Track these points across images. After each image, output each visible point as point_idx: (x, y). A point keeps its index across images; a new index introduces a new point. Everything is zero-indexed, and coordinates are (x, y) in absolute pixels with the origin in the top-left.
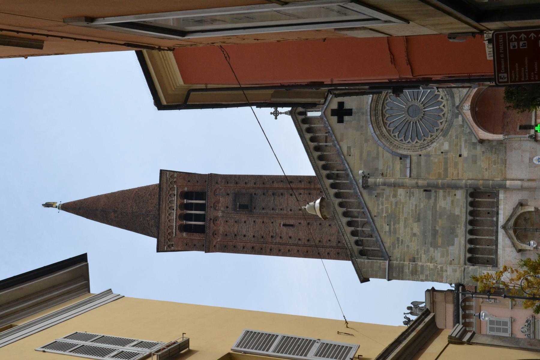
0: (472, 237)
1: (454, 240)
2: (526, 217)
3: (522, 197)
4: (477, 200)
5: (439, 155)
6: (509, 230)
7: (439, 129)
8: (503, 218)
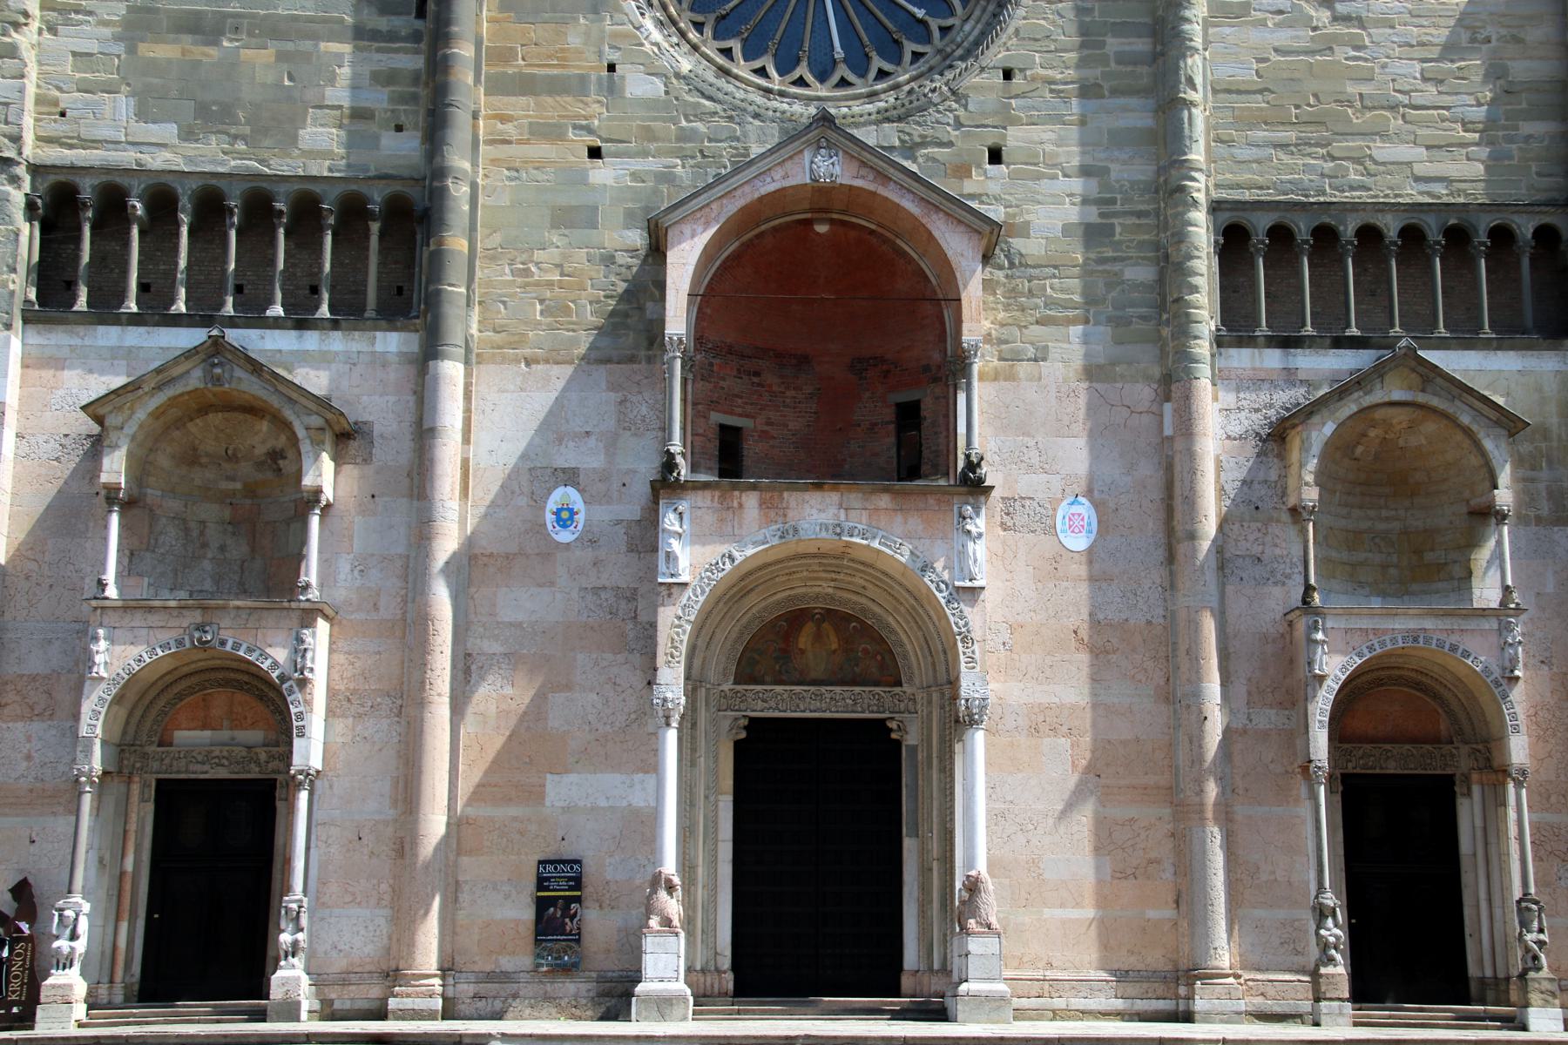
0: (185, 202)
1: (168, 121)
2: (285, 458)
3: (382, 436)
4: (375, 227)
5: (600, 54)
6: (204, 370)
7: (732, 60)
8: (280, 351)
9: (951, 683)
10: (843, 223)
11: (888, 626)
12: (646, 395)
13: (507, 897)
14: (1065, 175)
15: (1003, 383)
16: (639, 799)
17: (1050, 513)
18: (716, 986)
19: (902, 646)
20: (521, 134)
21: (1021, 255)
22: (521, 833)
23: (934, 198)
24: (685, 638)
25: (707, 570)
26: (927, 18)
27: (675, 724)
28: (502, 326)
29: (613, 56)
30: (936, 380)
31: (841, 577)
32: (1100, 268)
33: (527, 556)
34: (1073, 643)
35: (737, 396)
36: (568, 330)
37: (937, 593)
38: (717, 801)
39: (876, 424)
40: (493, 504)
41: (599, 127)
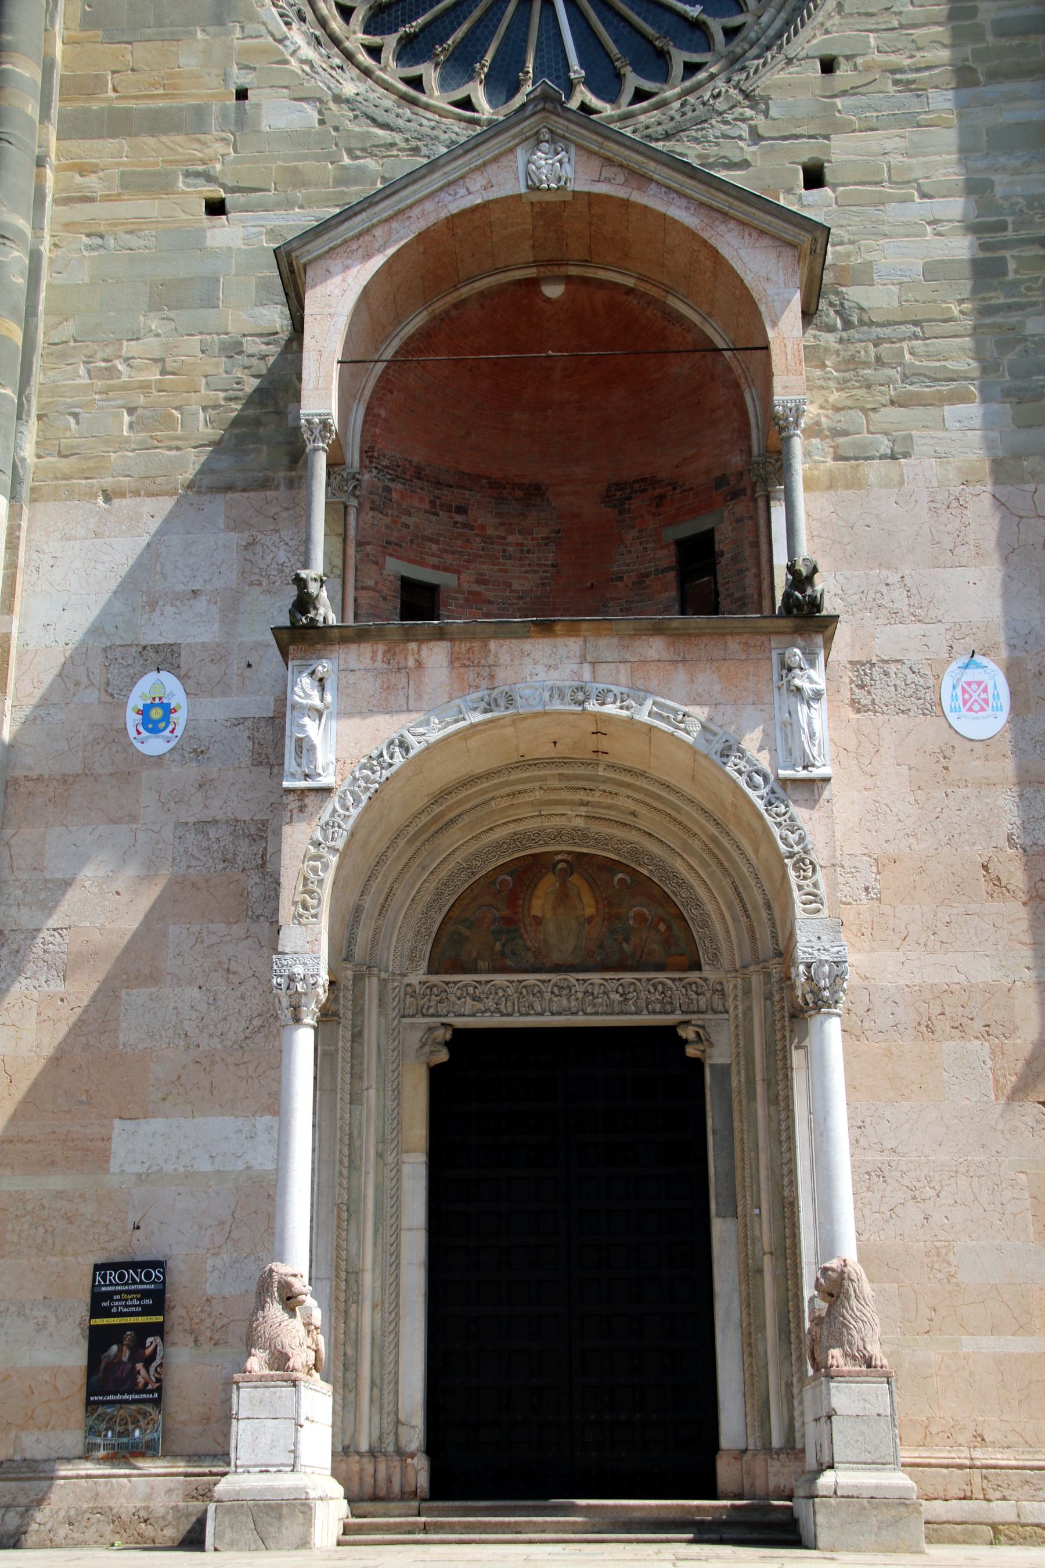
5: (226, 77)
9: (779, 954)
10: (586, 281)
11: (675, 875)
12: (286, 535)
13: (40, 1327)
14: (924, 195)
15: (843, 493)
16: (262, 1160)
17: (931, 682)
18: (396, 1480)
19: (699, 905)
20: (109, 189)
21: (861, 309)
22: (69, 1220)
23: (719, 200)
24: (329, 877)
25: (364, 767)
26: (704, 17)
27: (309, 1020)
28: (72, 447)
29: (244, 79)
30: (736, 495)
31: (596, 797)
32: (987, 321)
33: (96, 779)
34: (983, 886)
35: (431, 540)
36: (170, 449)
37: (749, 791)
38: (398, 1163)
39: (647, 575)
40: (44, 702)
41: (222, 172)
